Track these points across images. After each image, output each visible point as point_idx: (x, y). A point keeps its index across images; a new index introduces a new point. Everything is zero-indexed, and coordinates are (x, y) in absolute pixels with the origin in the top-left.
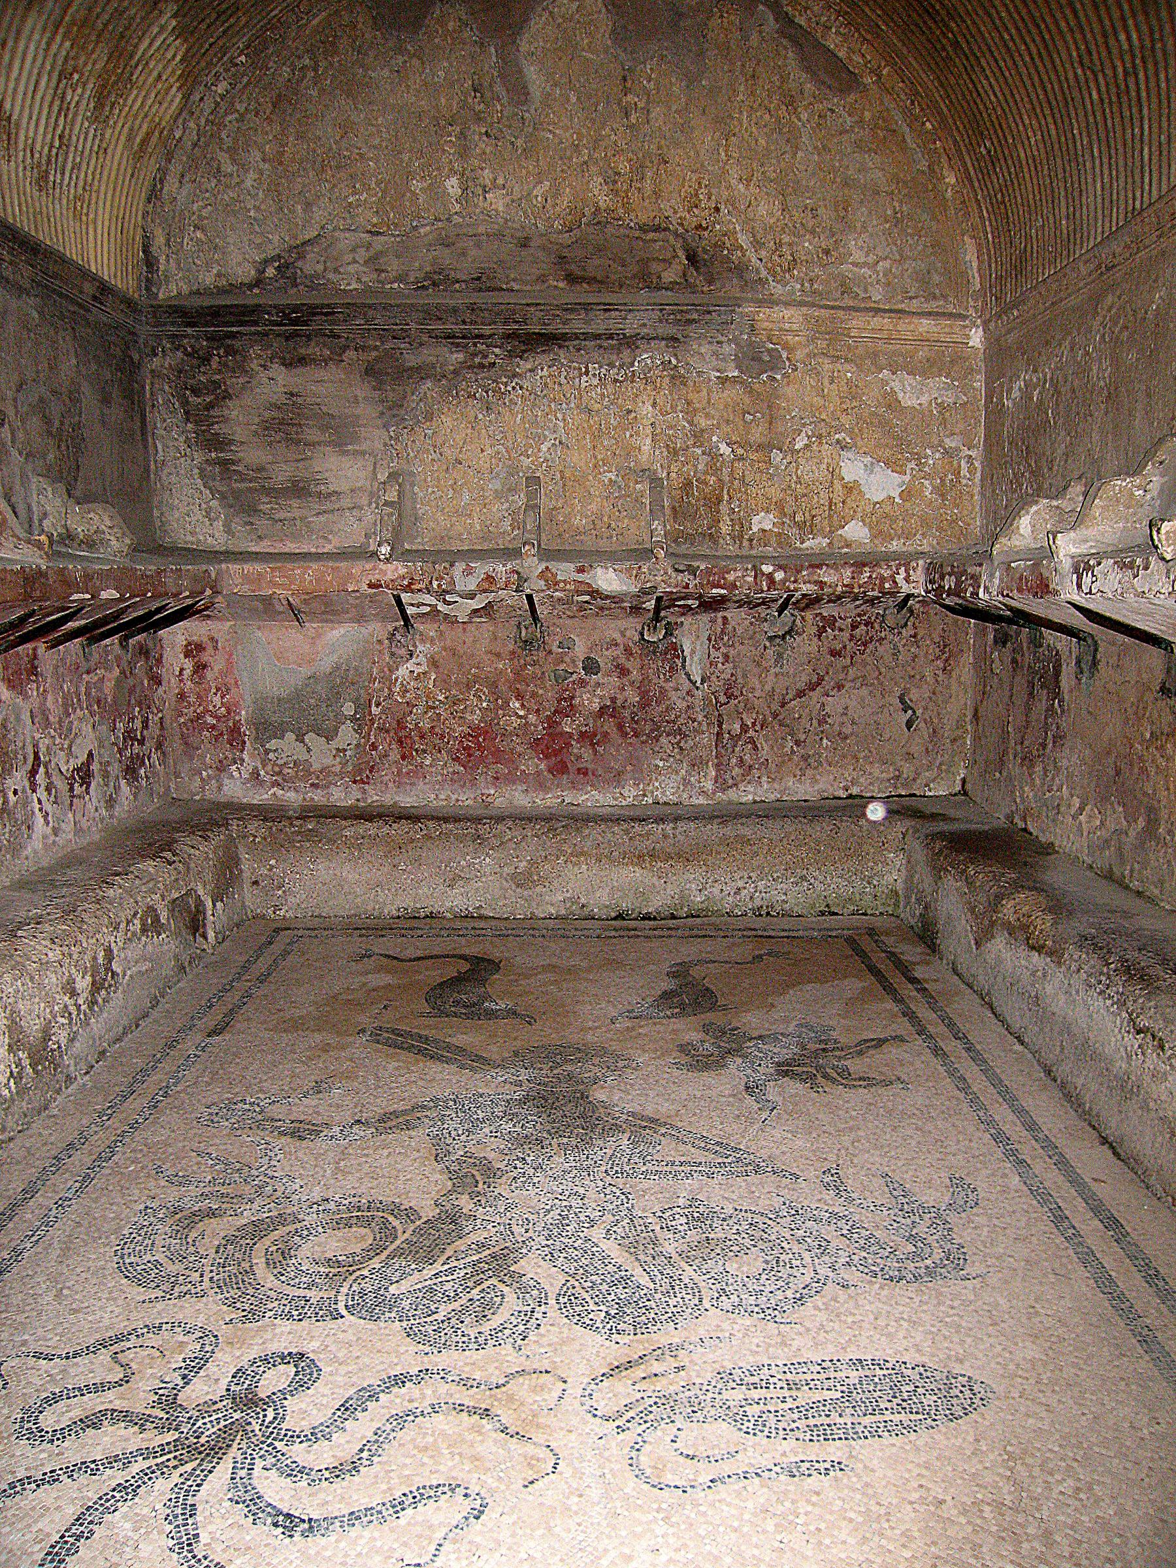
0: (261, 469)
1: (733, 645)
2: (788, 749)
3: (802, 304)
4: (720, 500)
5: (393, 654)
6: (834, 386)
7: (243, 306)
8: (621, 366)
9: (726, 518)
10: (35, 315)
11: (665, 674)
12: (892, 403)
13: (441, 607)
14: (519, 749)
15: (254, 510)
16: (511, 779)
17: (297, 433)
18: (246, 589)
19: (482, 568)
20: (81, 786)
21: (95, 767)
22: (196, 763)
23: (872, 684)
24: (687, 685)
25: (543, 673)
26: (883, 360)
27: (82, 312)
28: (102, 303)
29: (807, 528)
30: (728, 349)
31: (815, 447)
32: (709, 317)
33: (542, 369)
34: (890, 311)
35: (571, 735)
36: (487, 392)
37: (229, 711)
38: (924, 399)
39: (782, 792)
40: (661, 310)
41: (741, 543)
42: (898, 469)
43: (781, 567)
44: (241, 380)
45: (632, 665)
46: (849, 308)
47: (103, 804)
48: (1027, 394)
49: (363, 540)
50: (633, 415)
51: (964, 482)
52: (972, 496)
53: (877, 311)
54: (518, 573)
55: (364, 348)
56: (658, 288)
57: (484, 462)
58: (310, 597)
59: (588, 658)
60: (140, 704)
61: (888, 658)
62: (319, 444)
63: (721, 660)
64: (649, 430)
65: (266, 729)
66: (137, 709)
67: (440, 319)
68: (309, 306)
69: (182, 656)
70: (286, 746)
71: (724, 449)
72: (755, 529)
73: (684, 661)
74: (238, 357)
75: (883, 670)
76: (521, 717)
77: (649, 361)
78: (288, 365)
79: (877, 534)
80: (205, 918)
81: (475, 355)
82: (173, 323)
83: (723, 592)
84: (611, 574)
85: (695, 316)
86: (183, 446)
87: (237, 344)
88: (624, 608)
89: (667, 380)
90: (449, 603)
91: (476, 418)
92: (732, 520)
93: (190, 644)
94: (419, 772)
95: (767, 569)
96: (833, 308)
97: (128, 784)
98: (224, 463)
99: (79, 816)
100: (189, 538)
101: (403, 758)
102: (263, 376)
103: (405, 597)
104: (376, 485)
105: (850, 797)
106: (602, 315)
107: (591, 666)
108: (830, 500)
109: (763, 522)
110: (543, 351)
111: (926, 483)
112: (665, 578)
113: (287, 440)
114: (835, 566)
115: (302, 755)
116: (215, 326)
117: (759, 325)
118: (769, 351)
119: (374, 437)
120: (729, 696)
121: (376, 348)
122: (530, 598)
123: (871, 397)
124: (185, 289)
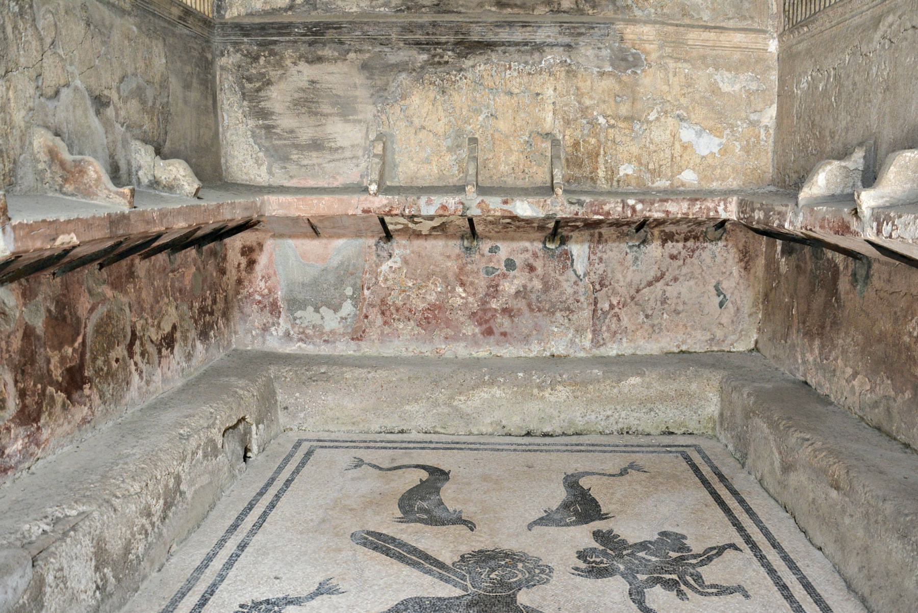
0: (292, 132)
1: (605, 252)
2: (640, 321)
3: (655, 22)
4: (598, 155)
5: (378, 256)
6: (676, 79)
7: (280, 23)
8: (533, 64)
9: (602, 167)
10: (135, 28)
11: (559, 271)
12: (715, 90)
13: (411, 225)
14: (462, 319)
15: (286, 159)
16: (455, 339)
17: (316, 108)
18: (280, 212)
19: (438, 200)
20: (167, 349)
21: (178, 335)
22: (248, 325)
23: (697, 278)
24: (574, 278)
25: (478, 269)
26: (709, 61)
27: (171, 27)
28: (186, 22)
29: (656, 173)
30: (606, 53)
31: (662, 119)
32: (592, 31)
33: (480, 65)
34: (715, 28)
35: (496, 310)
36: (442, 81)
37: (270, 291)
38: (737, 87)
39: (636, 348)
40: (560, 26)
41: (612, 183)
42: (718, 134)
43: (642, 201)
44: (279, 72)
45: (538, 264)
46: (688, 26)
47: (183, 359)
48: (813, 85)
49: (359, 179)
50: (540, 97)
51: (762, 143)
52: (767, 153)
53: (706, 28)
54: (462, 204)
55: (360, 51)
56: (558, 11)
57: (440, 127)
58: (323, 218)
59: (508, 259)
60: (210, 289)
61: (708, 261)
62: (331, 115)
63: (597, 261)
64: (551, 107)
65: (295, 304)
66: (208, 292)
67: (412, 32)
68: (325, 23)
69: (239, 255)
70: (308, 315)
71: (602, 120)
72: (621, 174)
73: (573, 260)
74: (278, 57)
75: (705, 268)
76: (463, 298)
77: (552, 61)
78: (310, 62)
79: (703, 178)
80: (251, 437)
81: (434, 56)
82: (235, 35)
83: (601, 217)
84: (526, 205)
85: (583, 30)
86: (240, 116)
87: (277, 48)
88: (534, 227)
89: (564, 74)
90: (416, 223)
91: (435, 98)
92: (606, 168)
93: (244, 247)
94: (397, 334)
95: (631, 202)
96: (677, 25)
97: (202, 343)
98: (268, 128)
99: (165, 369)
100: (244, 177)
101: (385, 323)
102: (293, 70)
103: (387, 219)
104: (368, 142)
105: (682, 352)
106: (521, 30)
107: (510, 264)
108: (672, 155)
109: (626, 170)
110: (481, 53)
111: (737, 144)
112: (562, 208)
113: (309, 112)
114: (677, 201)
115: (319, 322)
116: (262, 36)
117: (626, 37)
118: (633, 54)
119: (368, 111)
120: (602, 285)
121: (369, 51)
122: (471, 221)
123: (702, 84)
124: (243, 11)
